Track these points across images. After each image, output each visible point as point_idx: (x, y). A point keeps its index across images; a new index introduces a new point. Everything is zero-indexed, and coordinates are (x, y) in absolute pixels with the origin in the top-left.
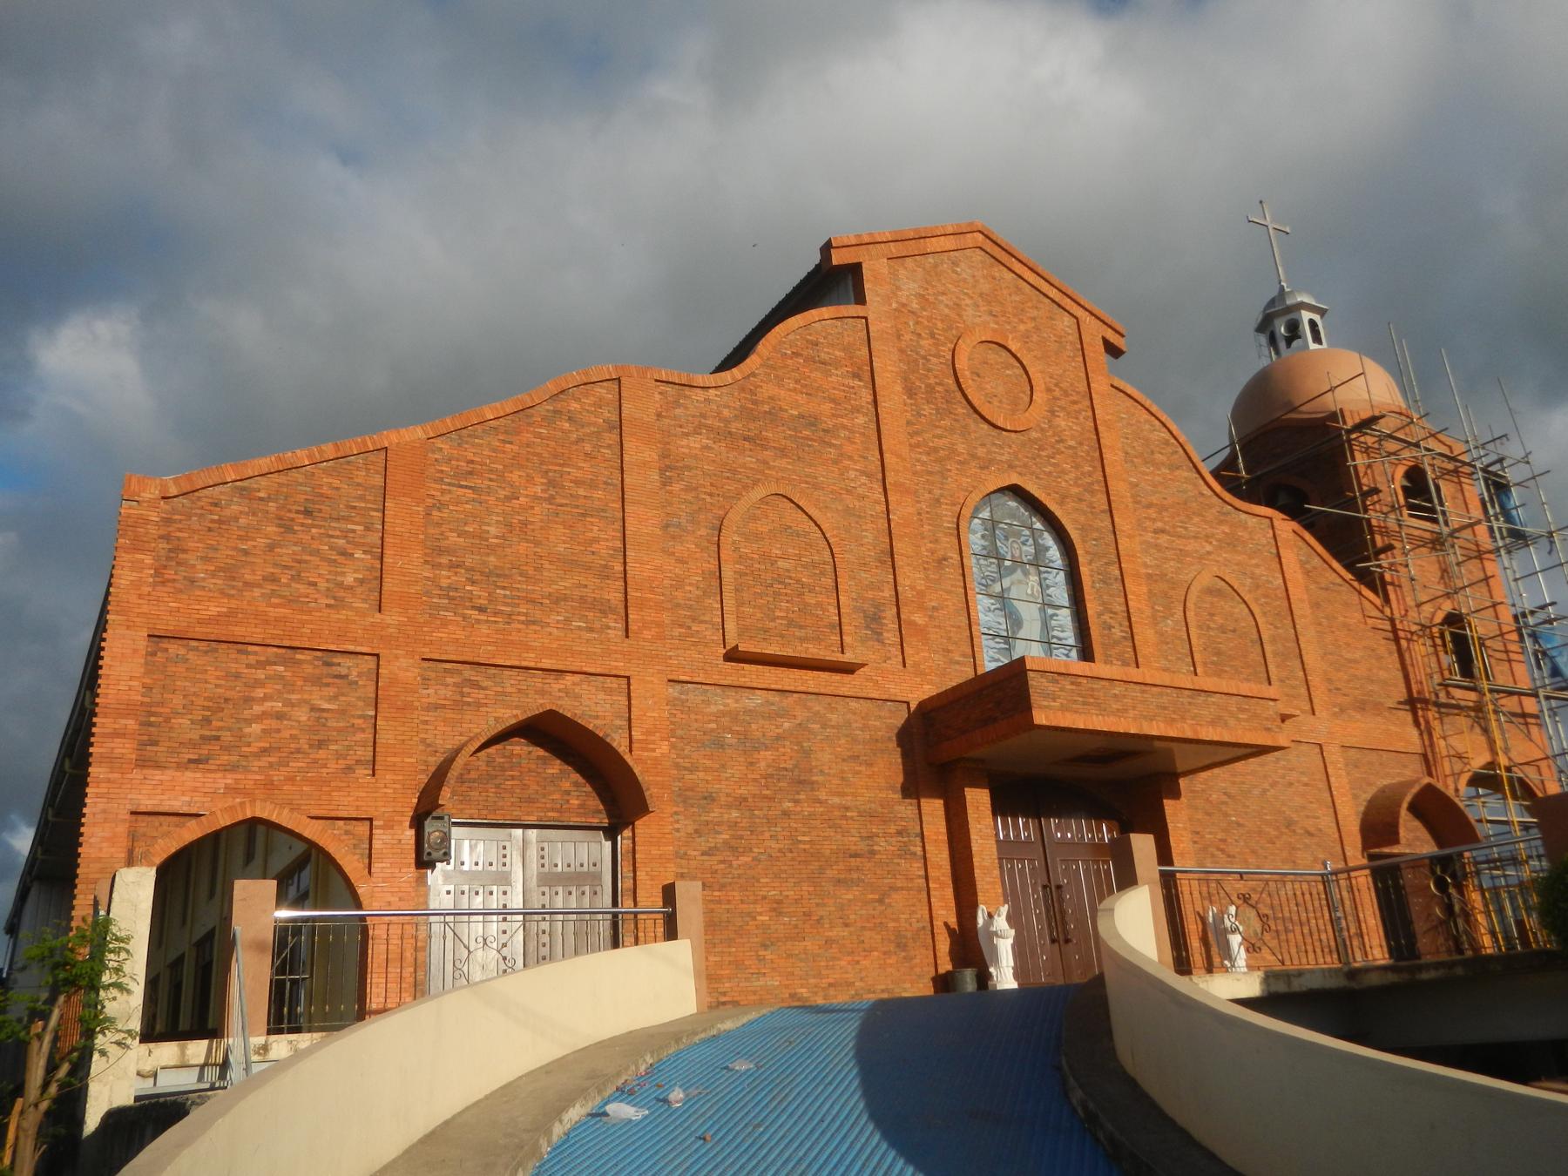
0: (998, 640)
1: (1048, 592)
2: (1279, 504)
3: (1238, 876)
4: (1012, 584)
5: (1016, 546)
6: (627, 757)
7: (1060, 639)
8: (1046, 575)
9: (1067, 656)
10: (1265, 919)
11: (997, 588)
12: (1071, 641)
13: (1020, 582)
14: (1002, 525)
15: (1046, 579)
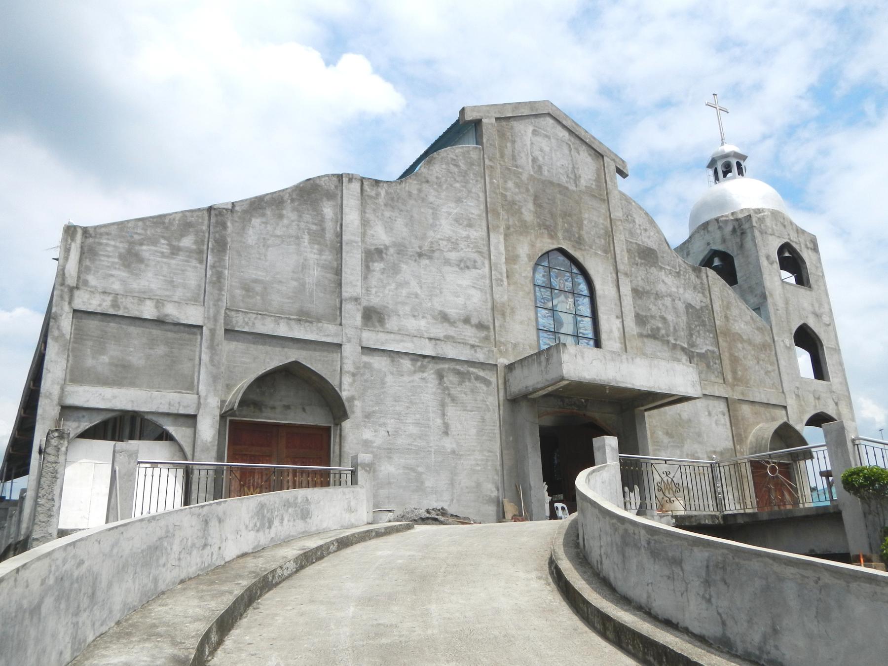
0: (549, 333)
1: (578, 308)
2: (715, 265)
3: (664, 462)
4: (559, 302)
5: (562, 281)
6: (337, 389)
7: (583, 334)
8: (578, 299)
9: (588, 344)
10: (677, 486)
11: (550, 305)
12: (591, 335)
13: (563, 302)
14: (554, 270)
15: (577, 301)
